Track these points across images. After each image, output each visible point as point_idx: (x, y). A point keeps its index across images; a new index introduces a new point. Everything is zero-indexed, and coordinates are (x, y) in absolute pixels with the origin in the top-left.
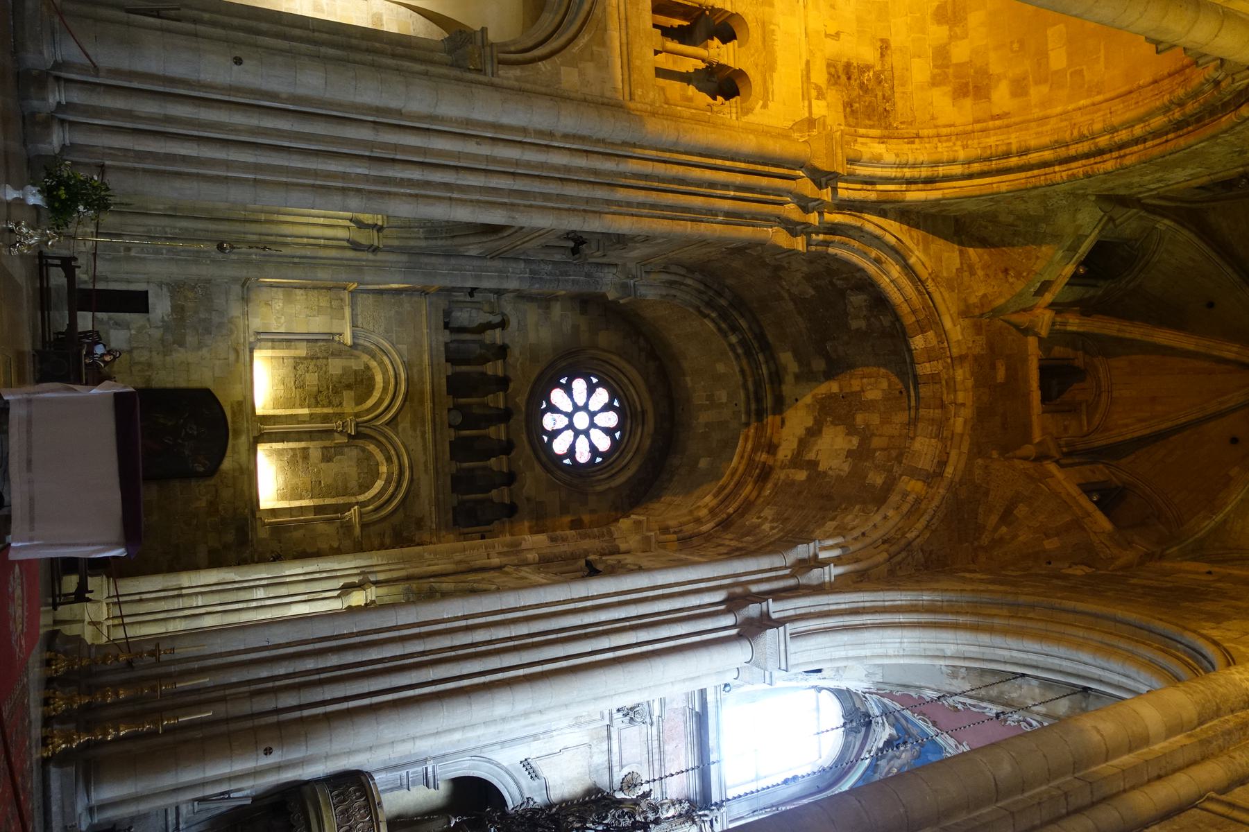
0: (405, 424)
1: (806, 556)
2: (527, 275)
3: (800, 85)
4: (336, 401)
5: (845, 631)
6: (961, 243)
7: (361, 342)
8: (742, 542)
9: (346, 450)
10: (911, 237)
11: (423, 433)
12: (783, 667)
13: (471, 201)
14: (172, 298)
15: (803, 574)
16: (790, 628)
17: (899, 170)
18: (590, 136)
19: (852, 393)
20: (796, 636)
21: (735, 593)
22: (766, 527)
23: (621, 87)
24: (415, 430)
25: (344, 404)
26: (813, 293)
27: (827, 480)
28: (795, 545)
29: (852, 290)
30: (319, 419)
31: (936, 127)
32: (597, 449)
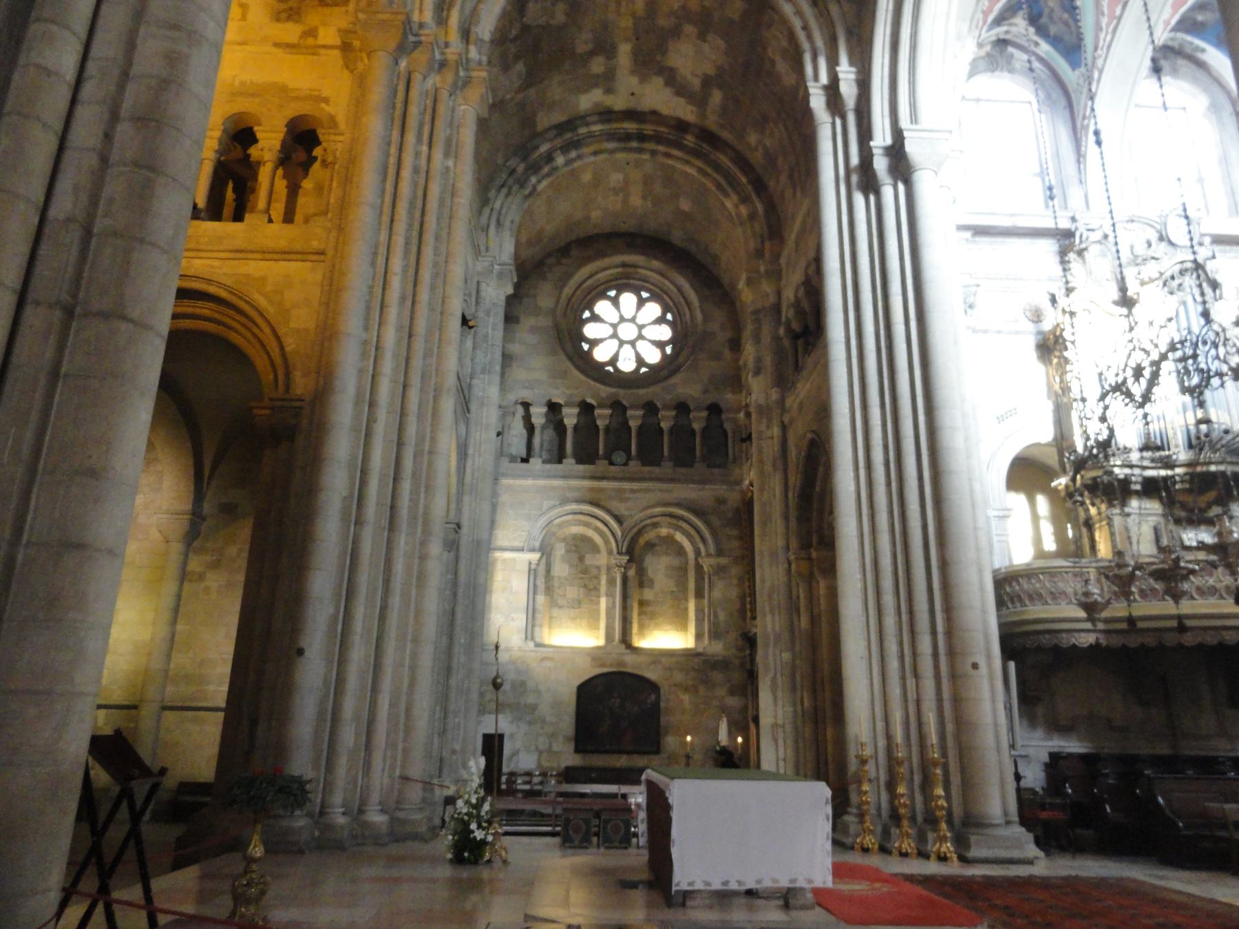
0: (621, 508)
3: (301, 57)
4: (595, 572)
11: (633, 491)
13: (432, 432)
16: (904, 122)
20: (914, 118)
21: (858, 183)
22: (768, 142)
24: (628, 499)
25: (598, 563)
29: (524, 16)
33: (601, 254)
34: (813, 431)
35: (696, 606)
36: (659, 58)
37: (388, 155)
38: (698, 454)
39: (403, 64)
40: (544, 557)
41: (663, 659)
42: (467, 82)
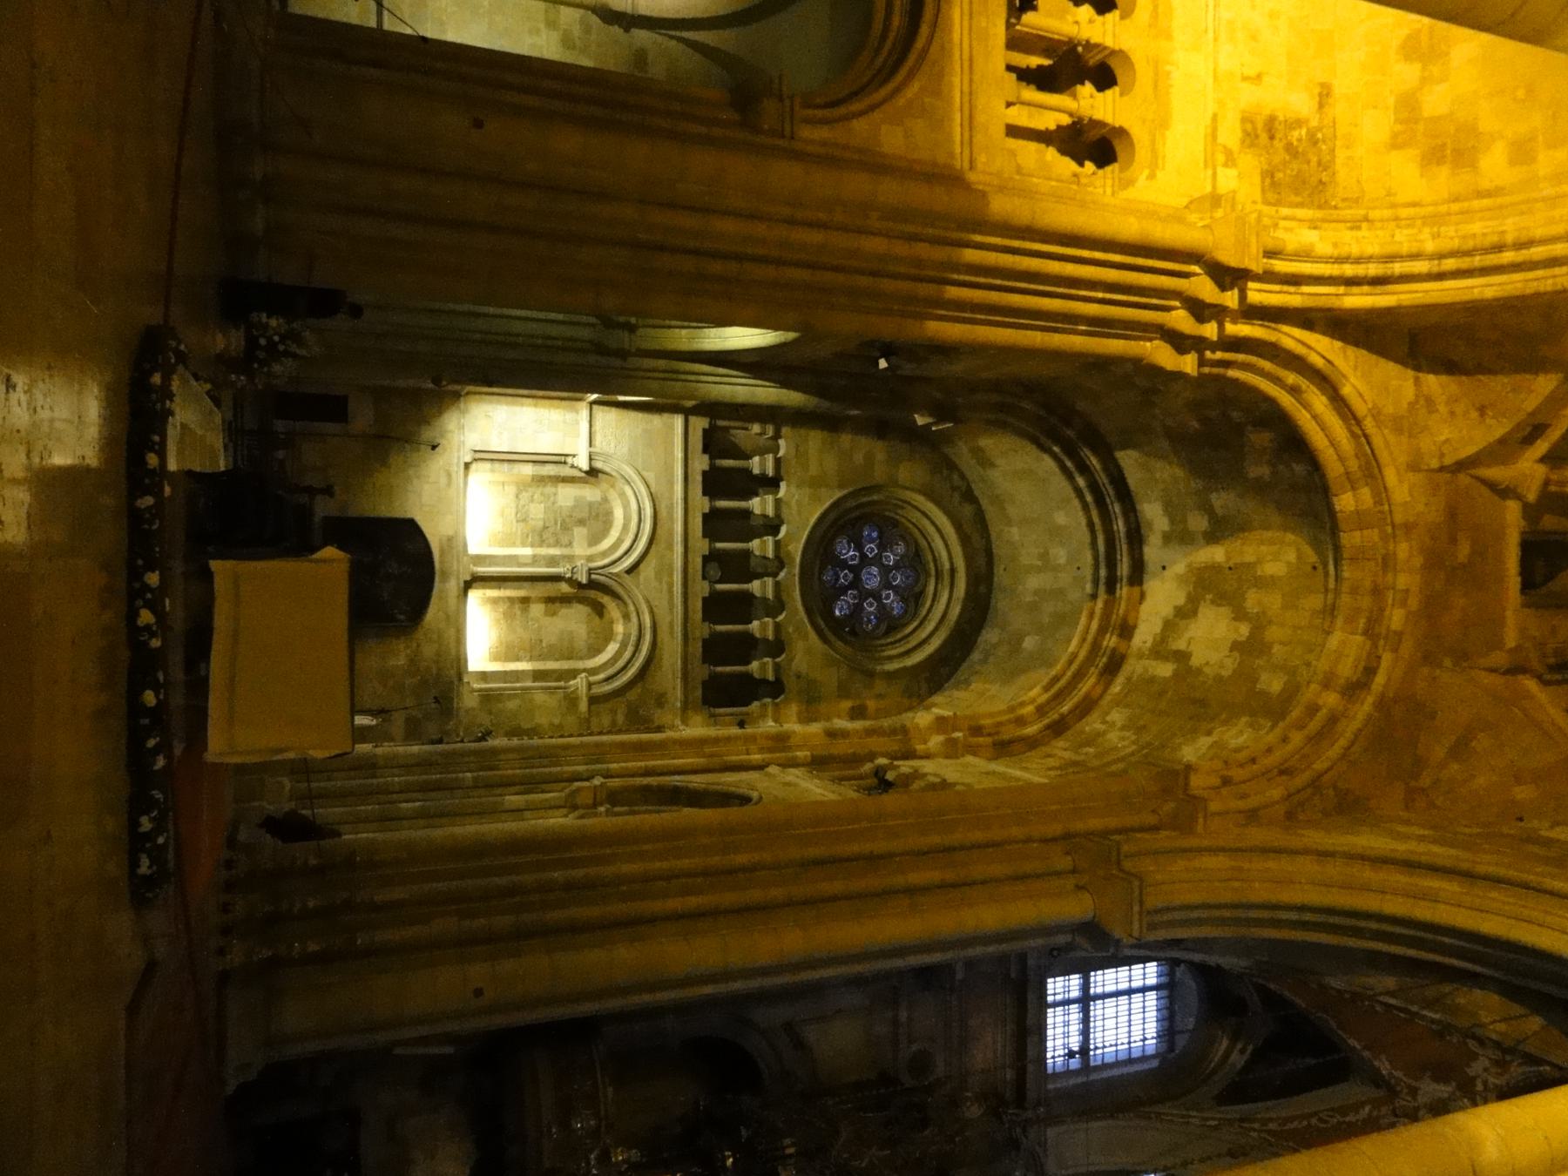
0: (648, 570)
4: (565, 540)
6: (1417, 368)
8: (1079, 754)
10: (1346, 357)
24: (661, 583)
25: (575, 544)
26: (1197, 425)
29: (1254, 426)
31: (1393, 206)
33: (965, 541)
34: (761, 798)
35: (523, 671)
38: (719, 669)
40: (583, 475)
41: (452, 632)
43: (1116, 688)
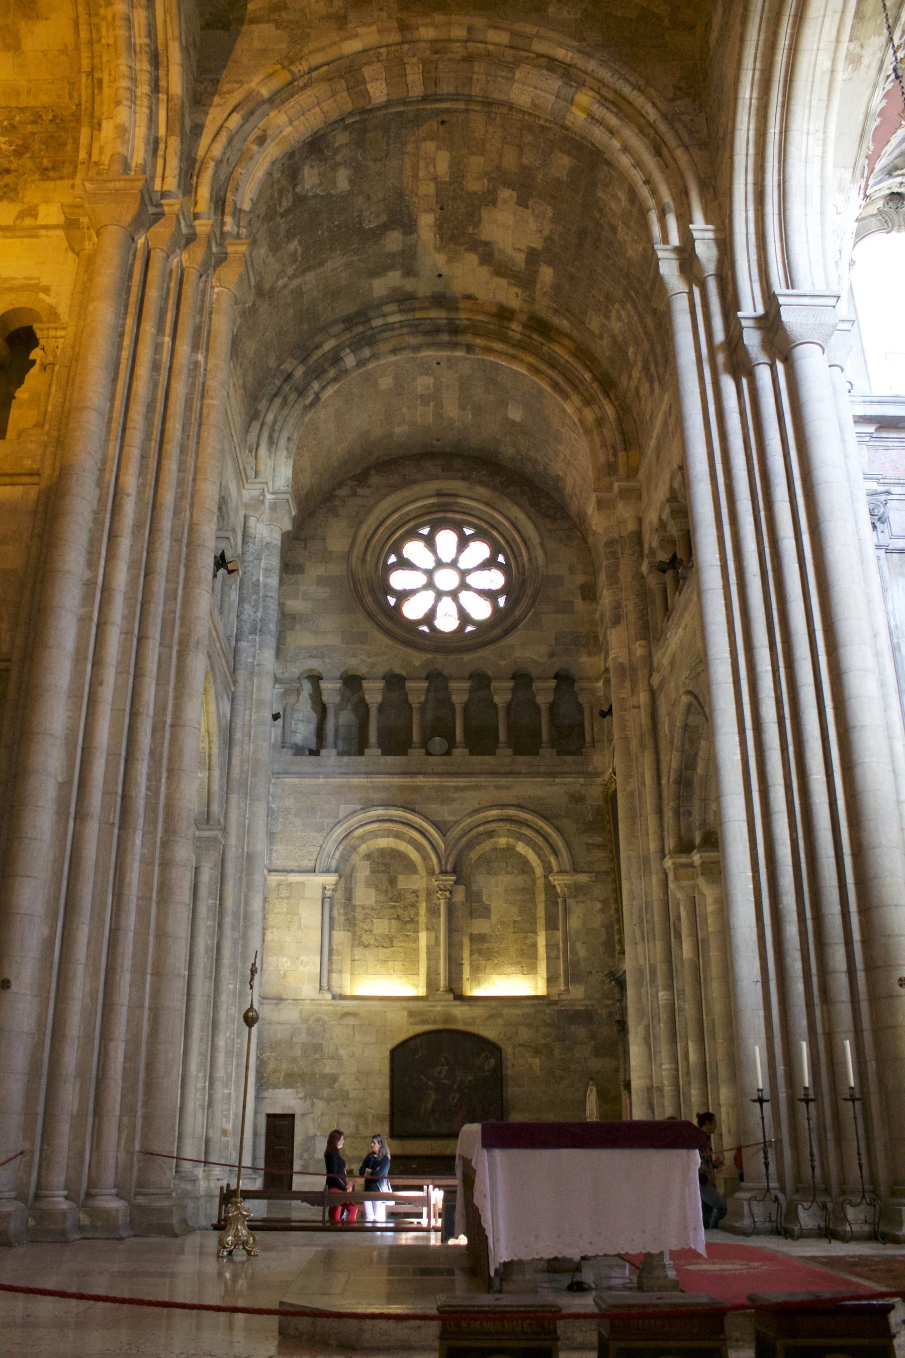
0: (445, 813)
1: (675, 264)
2: (257, 640)
4: (410, 898)
5: (788, 213)
6: (241, 21)
7: (334, 864)
8: (635, 361)
9: (475, 888)
10: (230, 92)
11: (457, 789)
12: (832, 301)
13: (176, 698)
14: (275, 1087)
15: (701, 269)
16: (778, 286)
17: (138, 103)
18: (90, 531)
19: (437, 195)
20: (790, 282)
21: (725, 365)
23: (21, 488)
24: (453, 800)
25: (415, 887)
26: (296, 242)
27: (556, 237)
28: (658, 279)
29: (296, 185)
30: (434, 920)
31: (77, 48)
32: (487, 560)
34: (689, 692)
35: (547, 940)
36: (470, 230)
37: (120, 347)
39: (141, 241)
40: (343, 879)
42: (222, 259)
43: (565, 324)
